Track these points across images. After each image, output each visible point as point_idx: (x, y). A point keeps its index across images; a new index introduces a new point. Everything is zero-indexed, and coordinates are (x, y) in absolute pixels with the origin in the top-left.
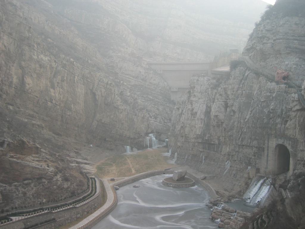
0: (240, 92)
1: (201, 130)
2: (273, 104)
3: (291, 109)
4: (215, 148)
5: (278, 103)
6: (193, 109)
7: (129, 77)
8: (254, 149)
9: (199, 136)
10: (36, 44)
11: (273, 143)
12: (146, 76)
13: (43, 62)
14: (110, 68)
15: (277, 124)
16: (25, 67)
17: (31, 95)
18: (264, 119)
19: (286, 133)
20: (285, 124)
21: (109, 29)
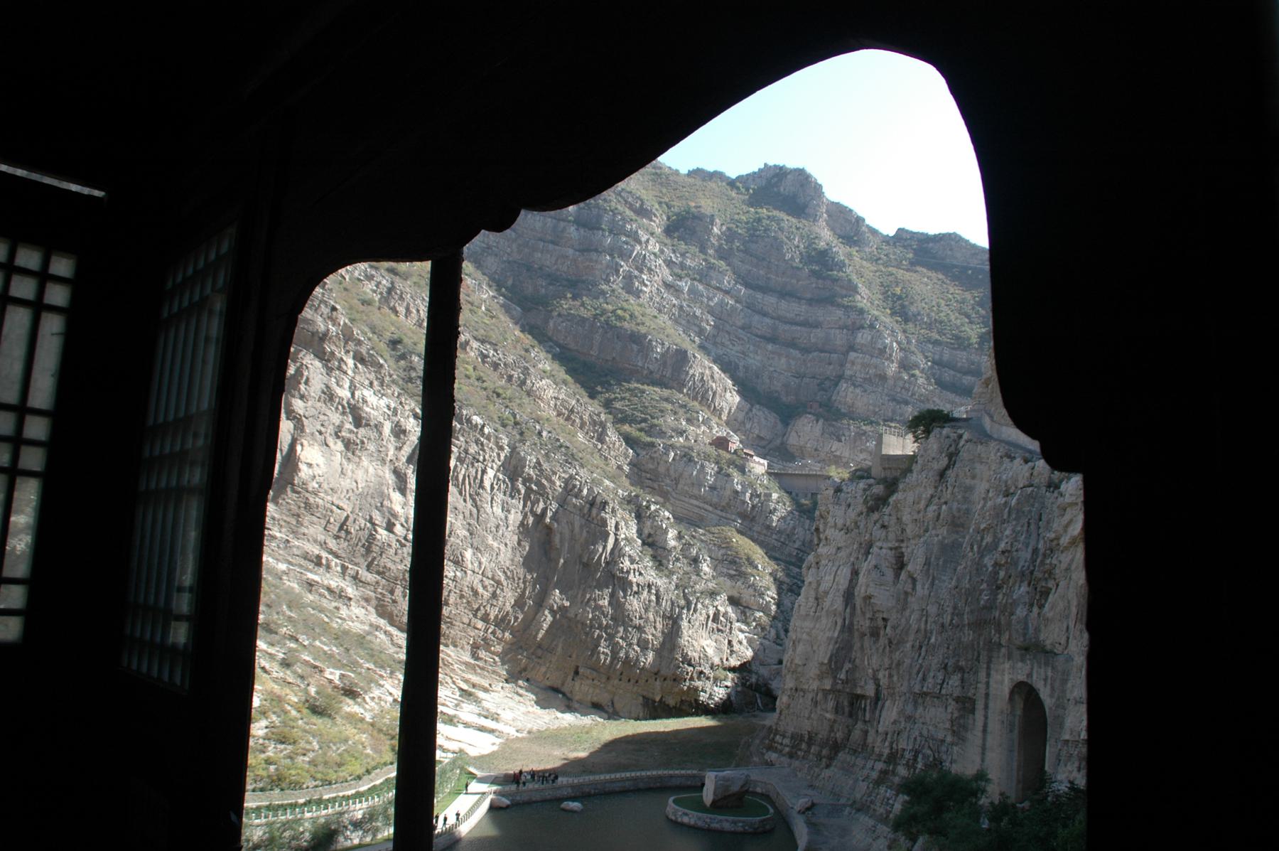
0: (932, 508)
1: (831, 647)
2: (1007, 532)
3: (1058, 538)
4: (868, 711)
5: (1022, 526)
6: (819, 585)
7: (702, 505)
8: (952, 706)
9: (824, 668)
10: (354, 358)
11: (1004, 677)
13: (367, 409)
14: (648, 476)
15: (1015, 604)
16: (305, 416)
17: (317, 499)
18: (983, 590)
19: (1042, 637)
20: (1041, 607)
21: (664, 373)
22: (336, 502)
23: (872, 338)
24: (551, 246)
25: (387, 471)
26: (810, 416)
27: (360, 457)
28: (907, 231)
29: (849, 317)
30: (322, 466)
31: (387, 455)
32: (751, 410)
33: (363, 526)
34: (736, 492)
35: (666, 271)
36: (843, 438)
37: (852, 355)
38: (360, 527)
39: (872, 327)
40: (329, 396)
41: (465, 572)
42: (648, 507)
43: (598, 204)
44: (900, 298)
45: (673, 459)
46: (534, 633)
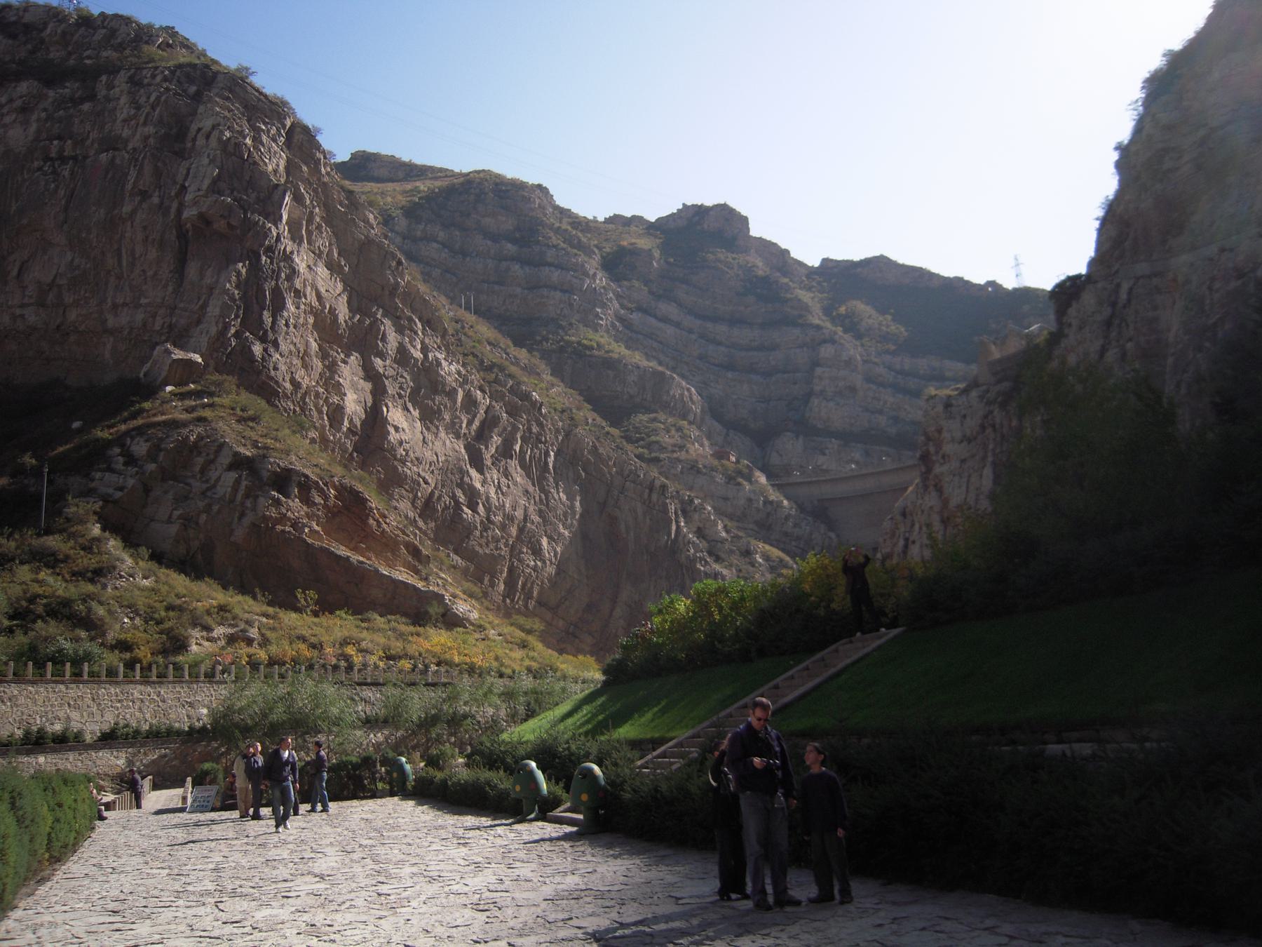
12: (768, 514)
13: (442, 373)
16: (384, 375)
17: (405, 469)
21: (645, 396)
22: (423, 474)
23: (836, 351)
24: (496, 287)
25: (462, 446)
26: (789, 434)
27: (437, 428)
28: (832, 260)
29: (806, 335)
30: (407, 431)
31: (461, 427)
32: (727, 435)
33: (448, 503)
34: (750, 500)
35: (617, 306)
36: (827, 451)
37: (819, 371)
38: (445, 504)
39: (833, 342)
40: (403, 357)
41: (544, 562)
42: (691, 501)
43: (539, 241)
44: (847, 316)
45: (682, 472)
46: (614, 631)
